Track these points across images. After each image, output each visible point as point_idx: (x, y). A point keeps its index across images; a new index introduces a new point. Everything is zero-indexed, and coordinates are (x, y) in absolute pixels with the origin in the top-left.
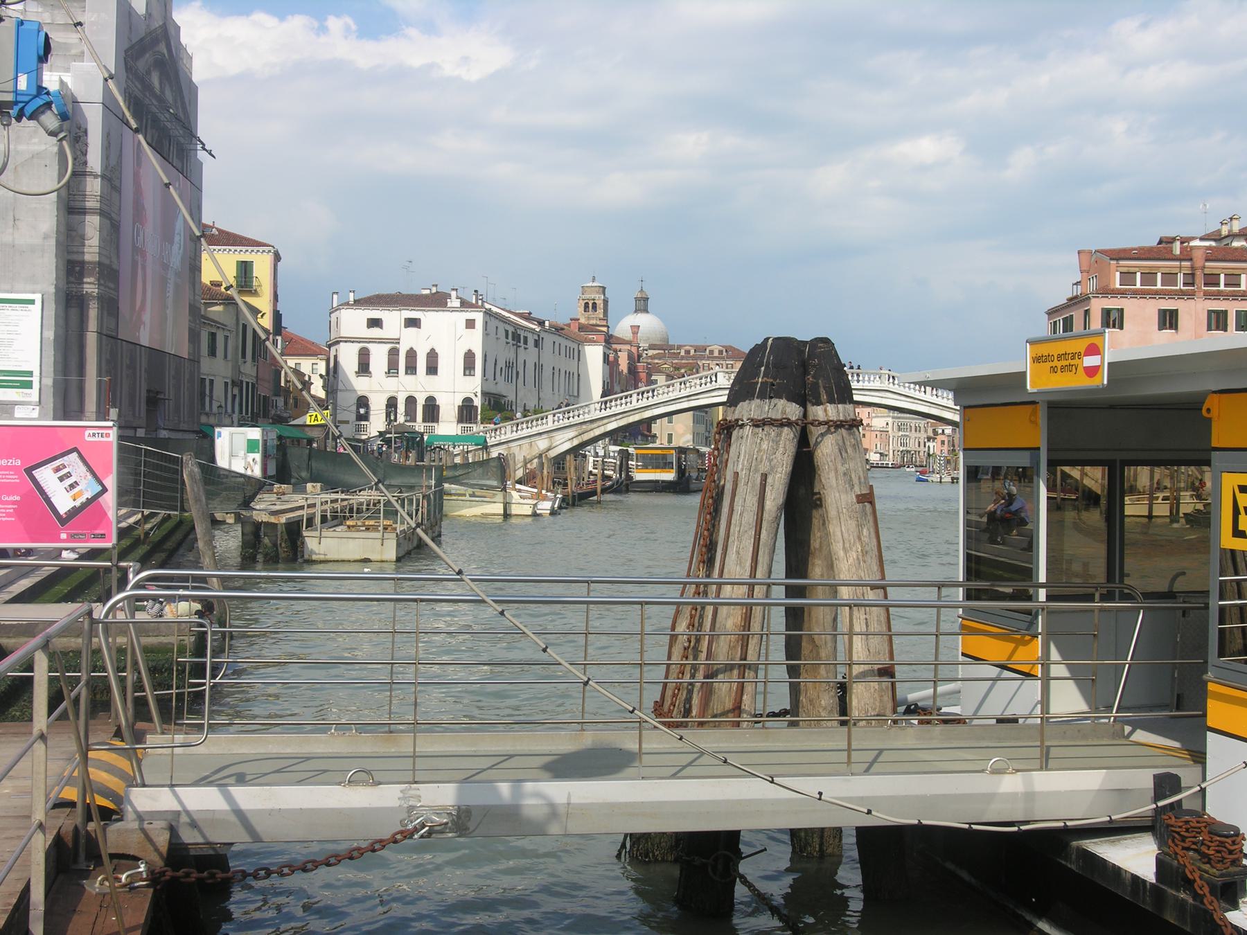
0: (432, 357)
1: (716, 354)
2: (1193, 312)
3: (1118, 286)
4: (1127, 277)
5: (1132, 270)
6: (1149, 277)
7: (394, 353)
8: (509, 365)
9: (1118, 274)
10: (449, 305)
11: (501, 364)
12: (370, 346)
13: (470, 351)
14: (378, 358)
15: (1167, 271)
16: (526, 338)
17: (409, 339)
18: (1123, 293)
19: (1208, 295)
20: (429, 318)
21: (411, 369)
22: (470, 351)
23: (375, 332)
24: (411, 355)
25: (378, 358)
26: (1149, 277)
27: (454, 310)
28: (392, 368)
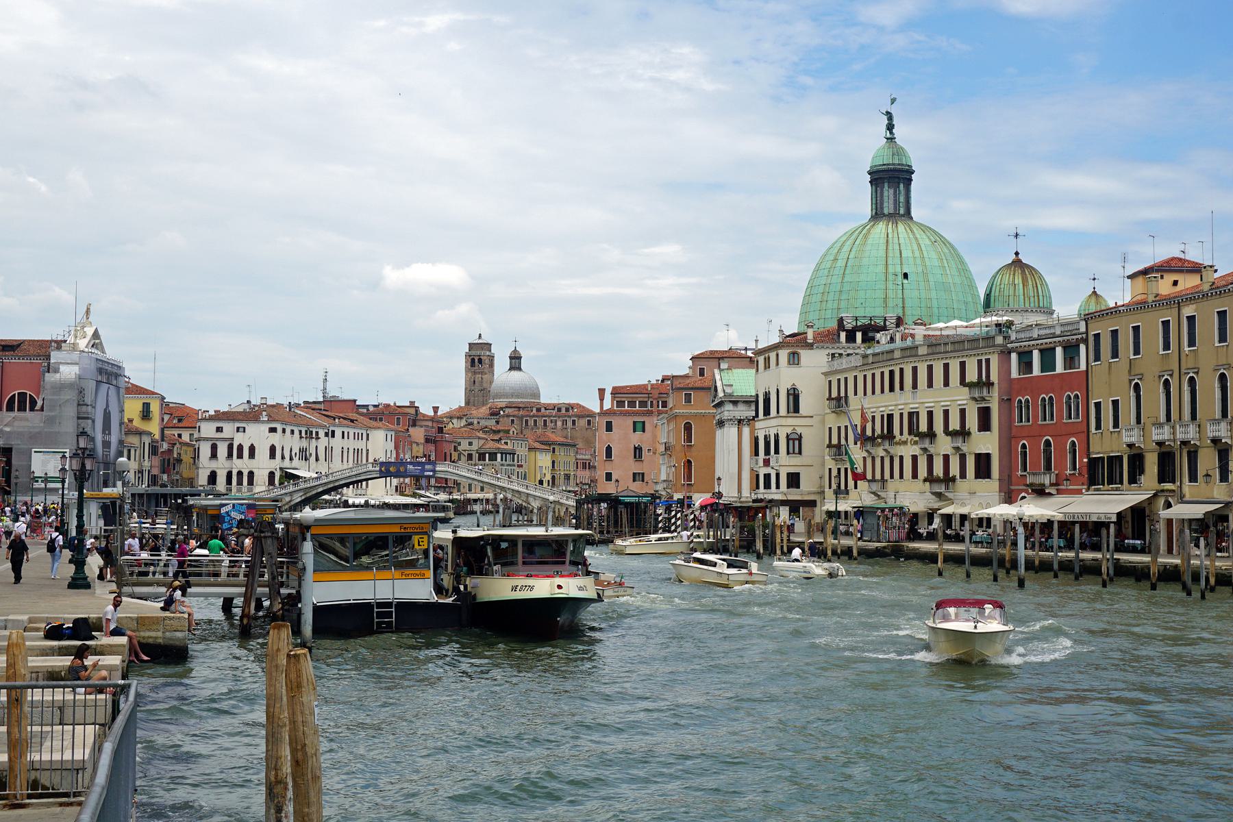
0: (252, 449)
1: (563, 411)
4: (621, 404)
6: (632, 404)
7: (230, 447)
8: (302, 451)
11: (296, 450)
14: (222, 450)
17: (239, 439)
20: (252, 428)
21: (240, 456)
24: (240, 448)
25: (222, 450)
26: (632, 404)
27: (263, 422)
28: (230, 455)
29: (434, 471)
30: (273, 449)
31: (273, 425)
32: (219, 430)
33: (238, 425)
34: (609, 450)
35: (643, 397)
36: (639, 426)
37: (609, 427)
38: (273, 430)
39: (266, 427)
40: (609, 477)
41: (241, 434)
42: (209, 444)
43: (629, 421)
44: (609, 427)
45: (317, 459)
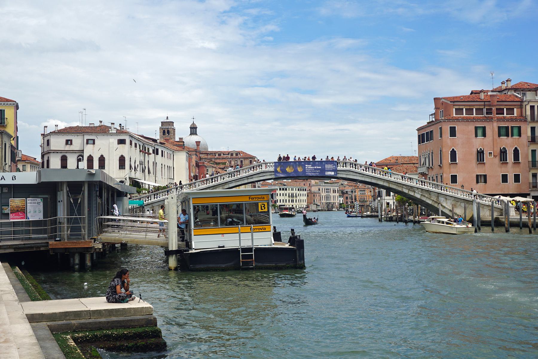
0: (102, 160)
2: (492, 128)
3: (454, 115)
5: (461, 107)
9: (454, 109)
10: (110, 132)
12: (67, 155)
13: (122, 156)
15: (478, 107)
16: (148, 149)
17: (89, 150)
18: (457, 120)
19: (499, 120)
22: (122, 156)
23: (68, 148)
24: (90, 159)
27: (112, 134)
29: (335, 171)
30: (122, 160)
31: (122, 137)
32: (69, 142)
33: (87, 137)
34: (453, 154)
35: (479, 105)
36: (480, 132)
37: (453, 132)
38: (122, 142)
39: (114, 140)
40: (454, 179)
41: (90, 146)
42: (59, 156)
43: (471, 128)
44: (453, 132)
45: (149, 172)
